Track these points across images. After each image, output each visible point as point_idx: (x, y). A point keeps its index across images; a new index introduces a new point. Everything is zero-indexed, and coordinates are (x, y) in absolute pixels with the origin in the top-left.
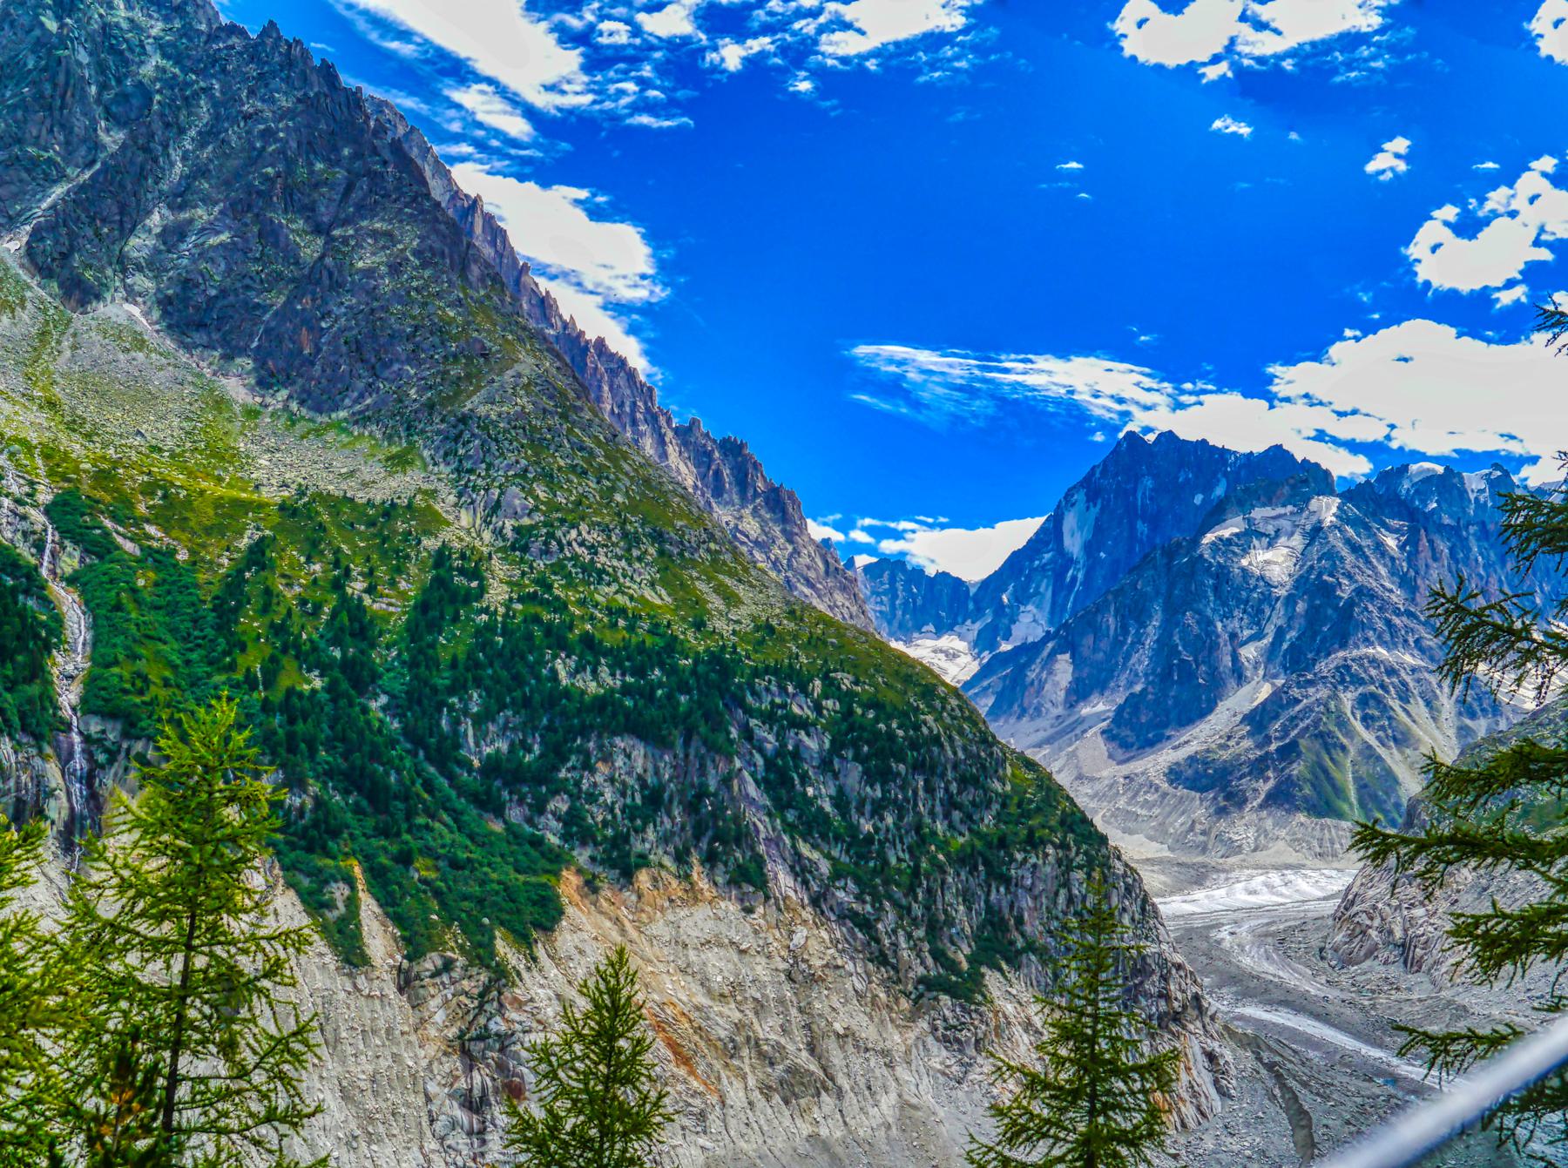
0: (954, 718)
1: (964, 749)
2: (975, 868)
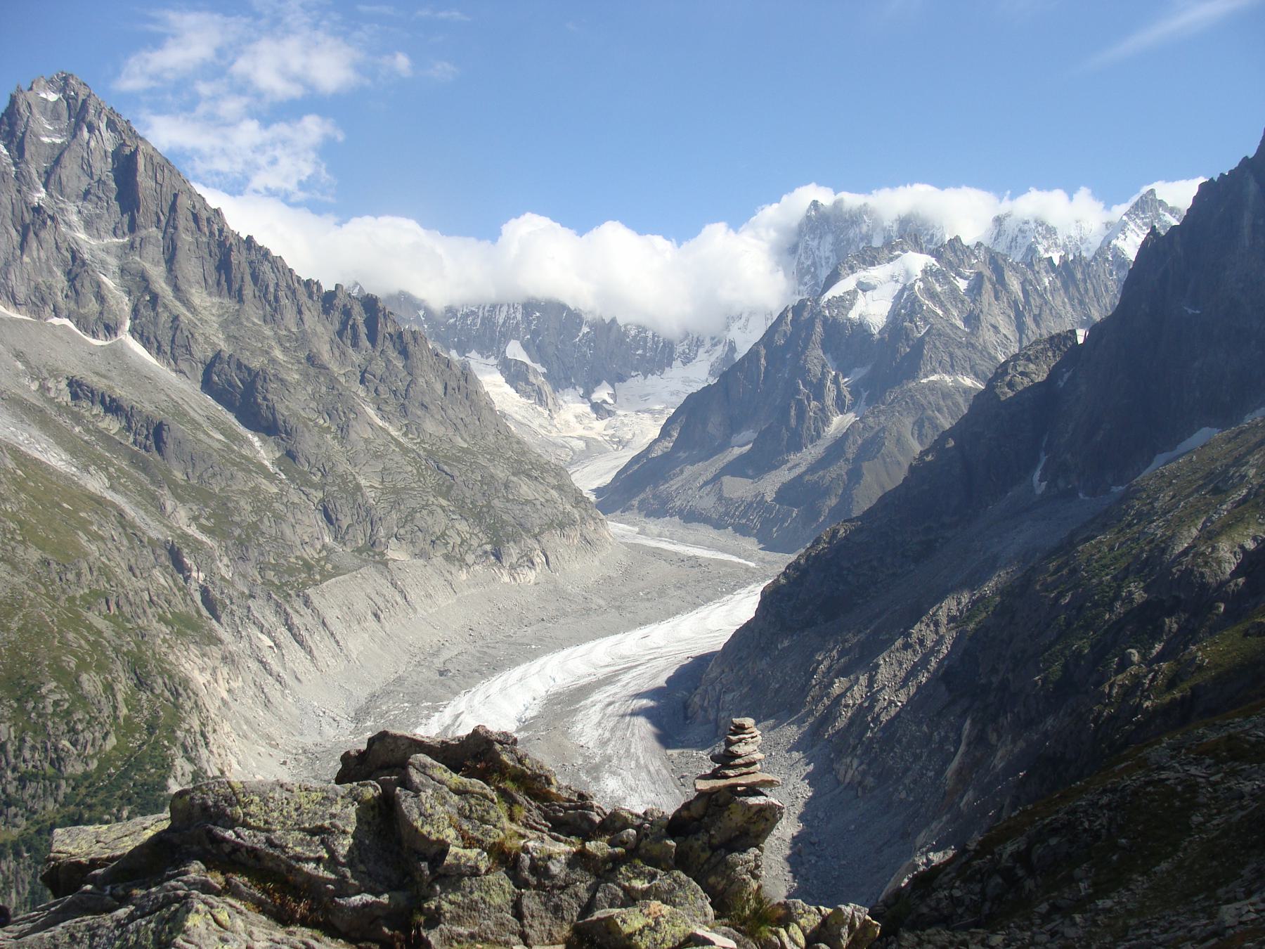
0: (39, 716)
1: (33, 748)
2: (18, 854)
